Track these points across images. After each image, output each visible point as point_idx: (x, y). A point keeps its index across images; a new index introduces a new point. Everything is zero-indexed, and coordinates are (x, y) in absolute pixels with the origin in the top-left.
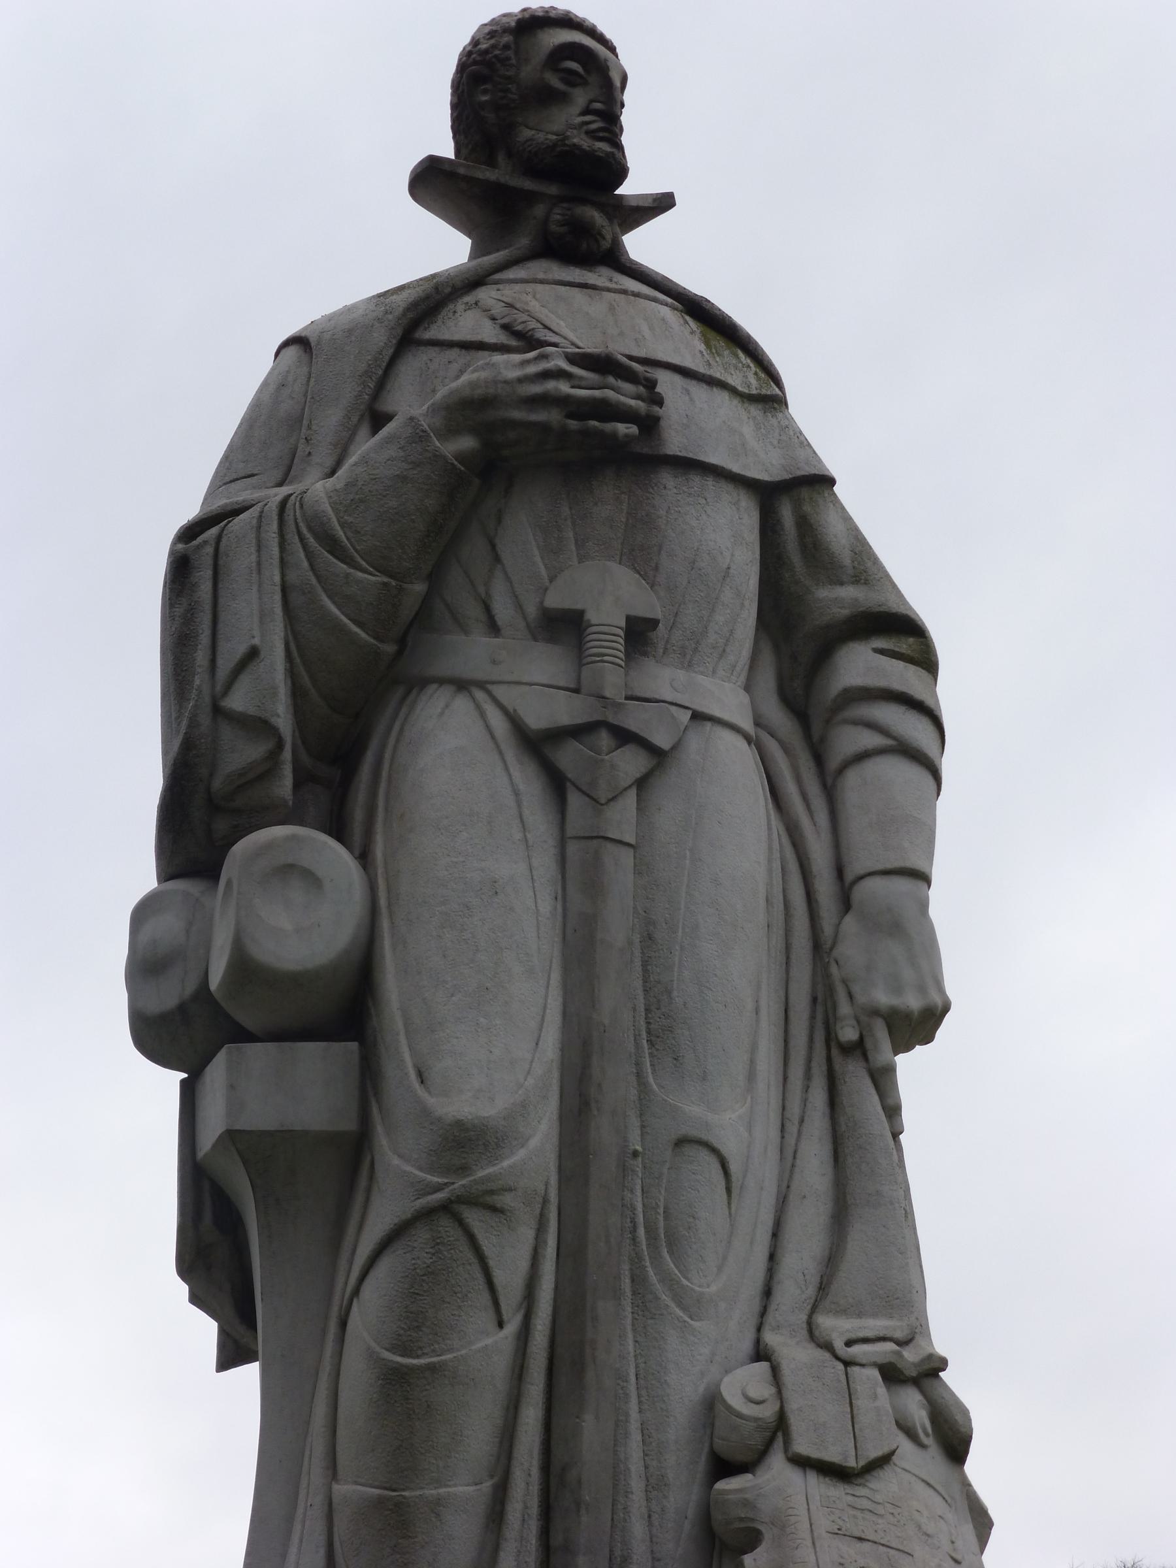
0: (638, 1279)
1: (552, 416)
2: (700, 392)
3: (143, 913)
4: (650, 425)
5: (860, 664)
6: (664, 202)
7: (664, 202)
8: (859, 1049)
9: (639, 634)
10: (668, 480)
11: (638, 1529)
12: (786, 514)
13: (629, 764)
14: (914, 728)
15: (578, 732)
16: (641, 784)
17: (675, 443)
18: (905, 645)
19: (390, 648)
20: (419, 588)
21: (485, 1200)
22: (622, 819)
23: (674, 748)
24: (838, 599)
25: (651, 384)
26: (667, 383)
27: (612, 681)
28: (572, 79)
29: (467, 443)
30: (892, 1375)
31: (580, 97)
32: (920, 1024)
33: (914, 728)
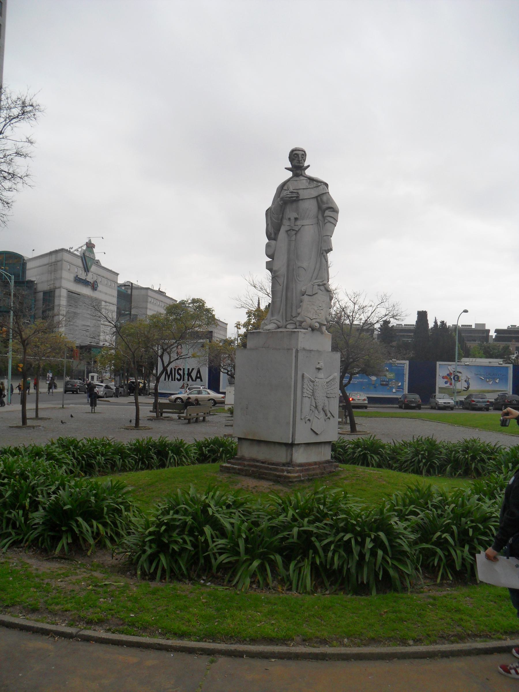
0: (295, 280)
1: (287, 199)
2: (305, 191)
3: (268, 246)
4: (297, 197)
5: (327, 213)
6: (309, 166)
7: (309, 166)
8: (323, 253)
9: (296, 219)
10: (300, 202)
11: (294, 302)
12: (319, 198)
13: (294, 232)
14: (332, 220)
15: (290, 230)
16: (296, 234)
17: (301, 198)
18: (331, 210)
19: (280, 221)
20: (281, 216)
21: (277, 276)
22: (293, 238)
23: (299, 229)
24: (324, 206)
25: (298, 193)
26: (300, 192)
27: (292, 225)
28: (296, 157)
29: (282, 202)
30: (319, 285)
31: (297, 159)
32: (331, 250)
33: (332, 220)
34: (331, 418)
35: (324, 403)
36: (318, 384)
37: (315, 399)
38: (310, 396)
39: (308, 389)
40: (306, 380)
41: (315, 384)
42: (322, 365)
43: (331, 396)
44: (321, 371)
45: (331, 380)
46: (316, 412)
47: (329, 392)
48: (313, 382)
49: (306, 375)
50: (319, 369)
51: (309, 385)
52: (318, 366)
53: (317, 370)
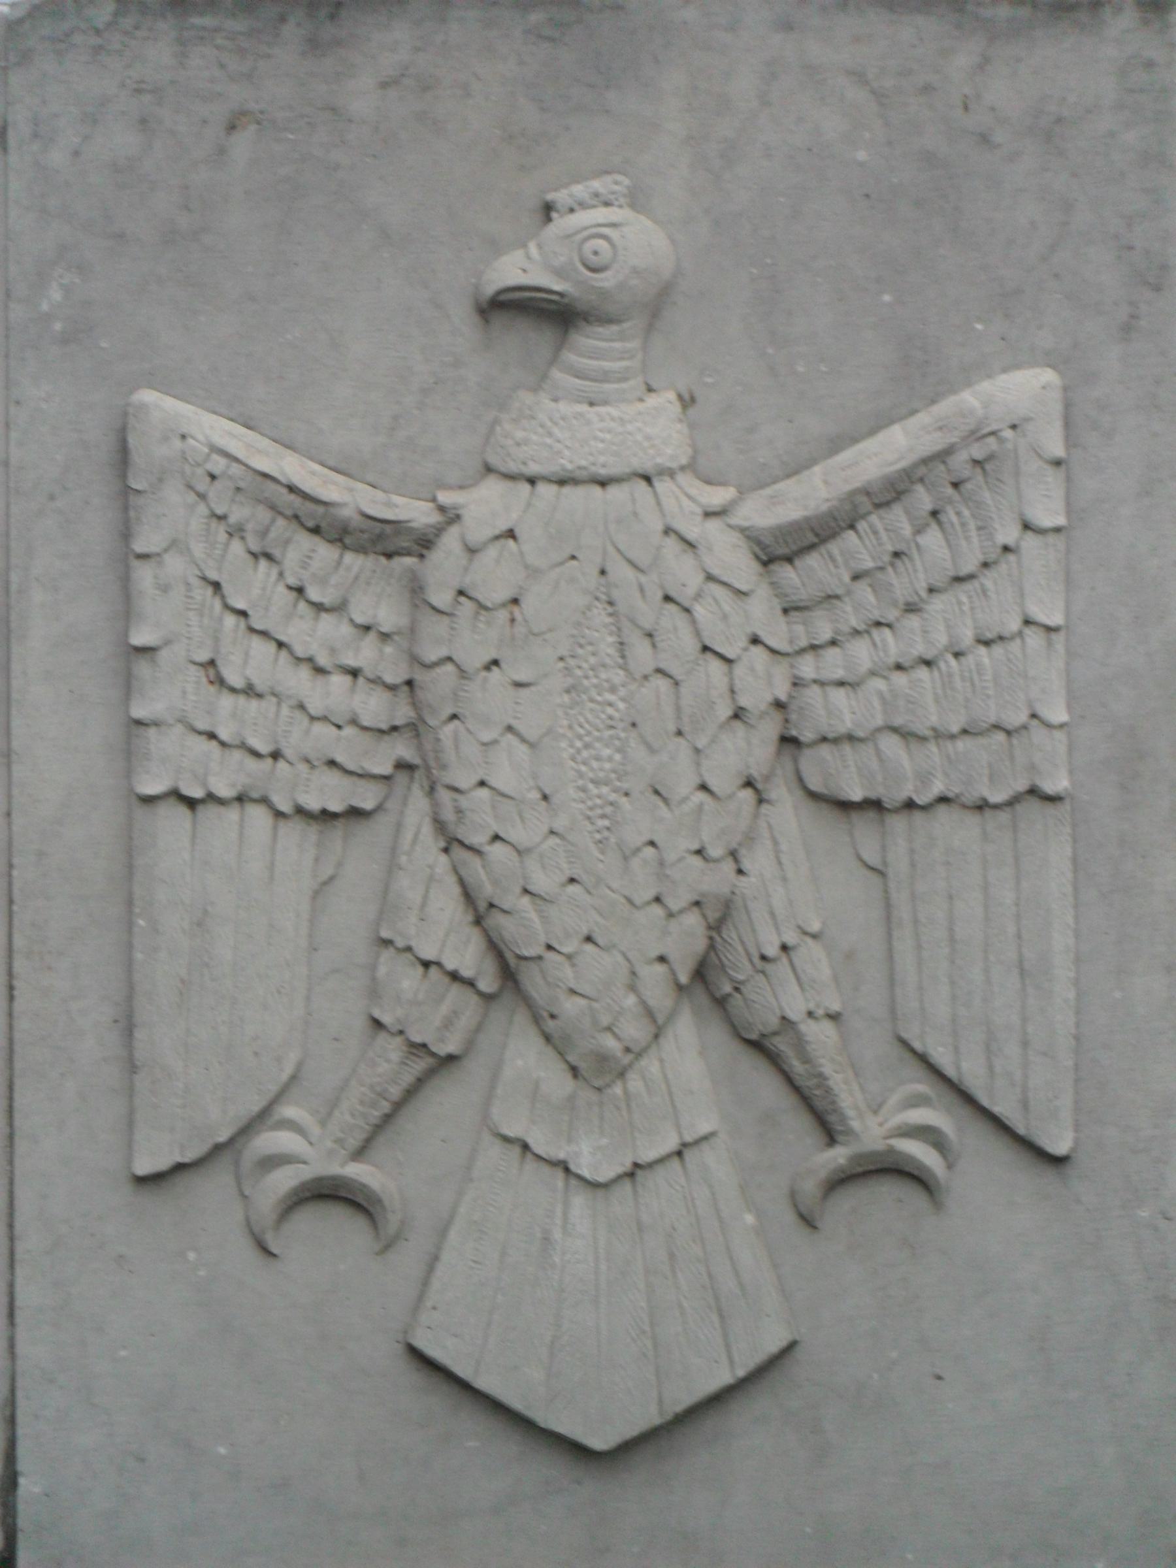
34: (981, 1176)
35: (720, 916)
36: (494, 577)
37: (451, 843)
38: (327, 792)
39: (250, 661)
40: (169, 516)
41: (444, 567)
42: (615, 232)
43: (903, 770)
44: (590, 346)
45: (891, 492)
46: (524, 1057)
47: (845, 711)
48: (384, 540)
49: (184, 422)
50: (552, 315)
51: (254, 586)
52: (513, 270)
53: (524, 338)
